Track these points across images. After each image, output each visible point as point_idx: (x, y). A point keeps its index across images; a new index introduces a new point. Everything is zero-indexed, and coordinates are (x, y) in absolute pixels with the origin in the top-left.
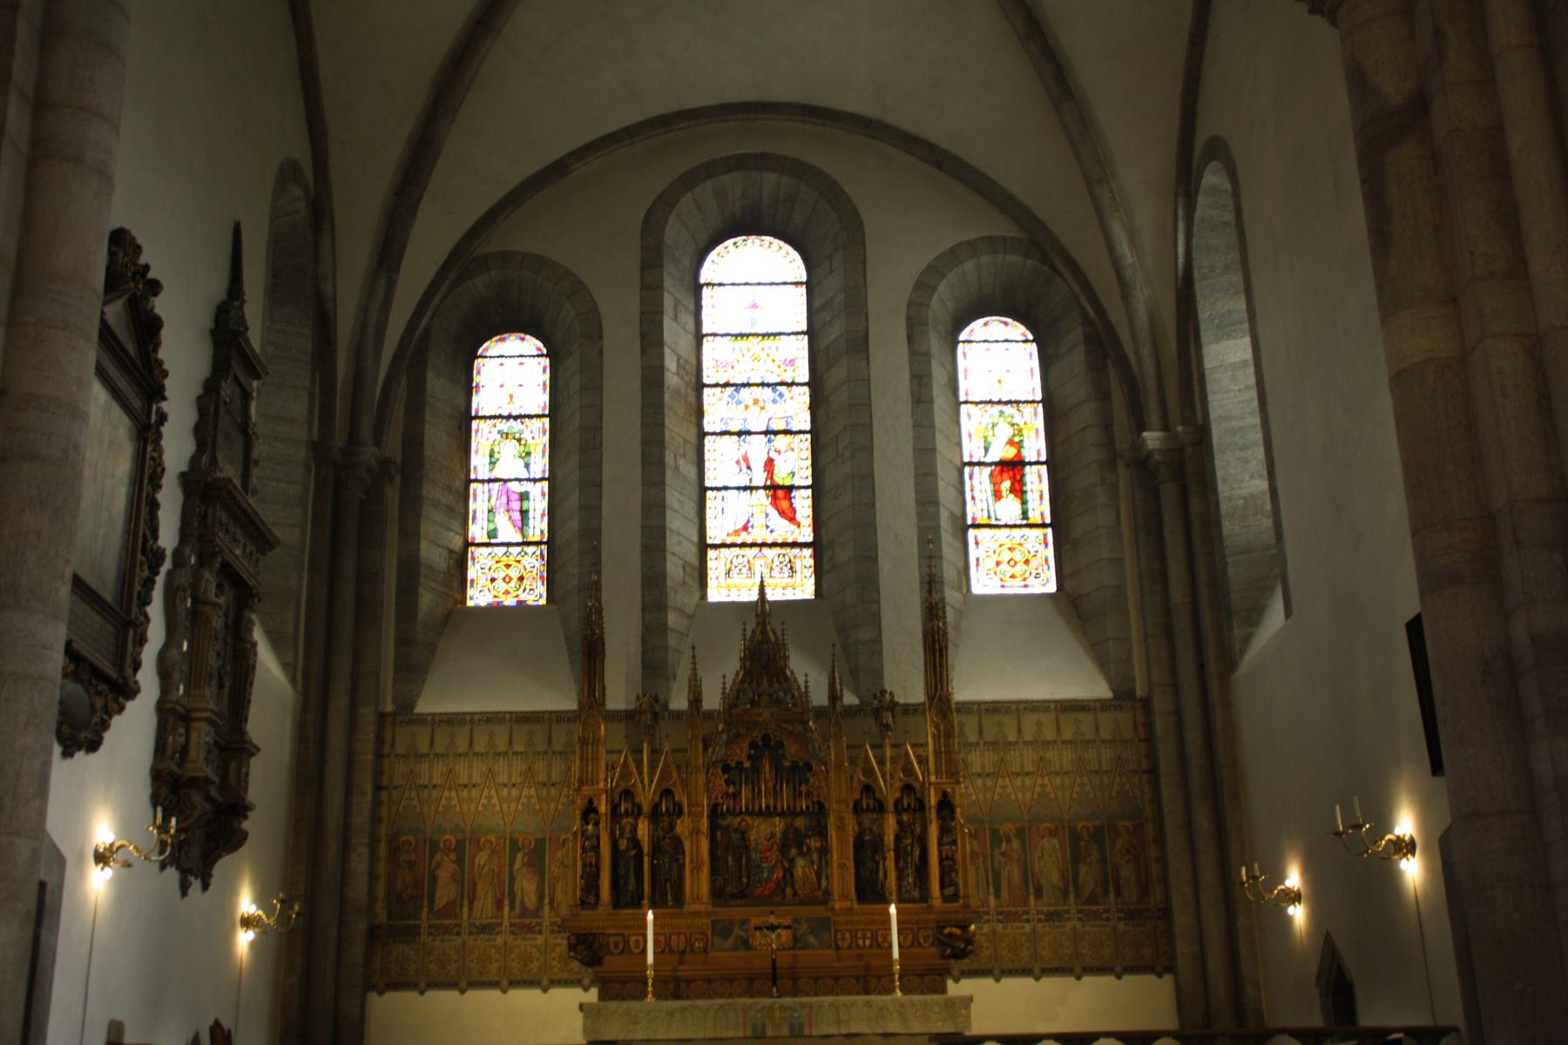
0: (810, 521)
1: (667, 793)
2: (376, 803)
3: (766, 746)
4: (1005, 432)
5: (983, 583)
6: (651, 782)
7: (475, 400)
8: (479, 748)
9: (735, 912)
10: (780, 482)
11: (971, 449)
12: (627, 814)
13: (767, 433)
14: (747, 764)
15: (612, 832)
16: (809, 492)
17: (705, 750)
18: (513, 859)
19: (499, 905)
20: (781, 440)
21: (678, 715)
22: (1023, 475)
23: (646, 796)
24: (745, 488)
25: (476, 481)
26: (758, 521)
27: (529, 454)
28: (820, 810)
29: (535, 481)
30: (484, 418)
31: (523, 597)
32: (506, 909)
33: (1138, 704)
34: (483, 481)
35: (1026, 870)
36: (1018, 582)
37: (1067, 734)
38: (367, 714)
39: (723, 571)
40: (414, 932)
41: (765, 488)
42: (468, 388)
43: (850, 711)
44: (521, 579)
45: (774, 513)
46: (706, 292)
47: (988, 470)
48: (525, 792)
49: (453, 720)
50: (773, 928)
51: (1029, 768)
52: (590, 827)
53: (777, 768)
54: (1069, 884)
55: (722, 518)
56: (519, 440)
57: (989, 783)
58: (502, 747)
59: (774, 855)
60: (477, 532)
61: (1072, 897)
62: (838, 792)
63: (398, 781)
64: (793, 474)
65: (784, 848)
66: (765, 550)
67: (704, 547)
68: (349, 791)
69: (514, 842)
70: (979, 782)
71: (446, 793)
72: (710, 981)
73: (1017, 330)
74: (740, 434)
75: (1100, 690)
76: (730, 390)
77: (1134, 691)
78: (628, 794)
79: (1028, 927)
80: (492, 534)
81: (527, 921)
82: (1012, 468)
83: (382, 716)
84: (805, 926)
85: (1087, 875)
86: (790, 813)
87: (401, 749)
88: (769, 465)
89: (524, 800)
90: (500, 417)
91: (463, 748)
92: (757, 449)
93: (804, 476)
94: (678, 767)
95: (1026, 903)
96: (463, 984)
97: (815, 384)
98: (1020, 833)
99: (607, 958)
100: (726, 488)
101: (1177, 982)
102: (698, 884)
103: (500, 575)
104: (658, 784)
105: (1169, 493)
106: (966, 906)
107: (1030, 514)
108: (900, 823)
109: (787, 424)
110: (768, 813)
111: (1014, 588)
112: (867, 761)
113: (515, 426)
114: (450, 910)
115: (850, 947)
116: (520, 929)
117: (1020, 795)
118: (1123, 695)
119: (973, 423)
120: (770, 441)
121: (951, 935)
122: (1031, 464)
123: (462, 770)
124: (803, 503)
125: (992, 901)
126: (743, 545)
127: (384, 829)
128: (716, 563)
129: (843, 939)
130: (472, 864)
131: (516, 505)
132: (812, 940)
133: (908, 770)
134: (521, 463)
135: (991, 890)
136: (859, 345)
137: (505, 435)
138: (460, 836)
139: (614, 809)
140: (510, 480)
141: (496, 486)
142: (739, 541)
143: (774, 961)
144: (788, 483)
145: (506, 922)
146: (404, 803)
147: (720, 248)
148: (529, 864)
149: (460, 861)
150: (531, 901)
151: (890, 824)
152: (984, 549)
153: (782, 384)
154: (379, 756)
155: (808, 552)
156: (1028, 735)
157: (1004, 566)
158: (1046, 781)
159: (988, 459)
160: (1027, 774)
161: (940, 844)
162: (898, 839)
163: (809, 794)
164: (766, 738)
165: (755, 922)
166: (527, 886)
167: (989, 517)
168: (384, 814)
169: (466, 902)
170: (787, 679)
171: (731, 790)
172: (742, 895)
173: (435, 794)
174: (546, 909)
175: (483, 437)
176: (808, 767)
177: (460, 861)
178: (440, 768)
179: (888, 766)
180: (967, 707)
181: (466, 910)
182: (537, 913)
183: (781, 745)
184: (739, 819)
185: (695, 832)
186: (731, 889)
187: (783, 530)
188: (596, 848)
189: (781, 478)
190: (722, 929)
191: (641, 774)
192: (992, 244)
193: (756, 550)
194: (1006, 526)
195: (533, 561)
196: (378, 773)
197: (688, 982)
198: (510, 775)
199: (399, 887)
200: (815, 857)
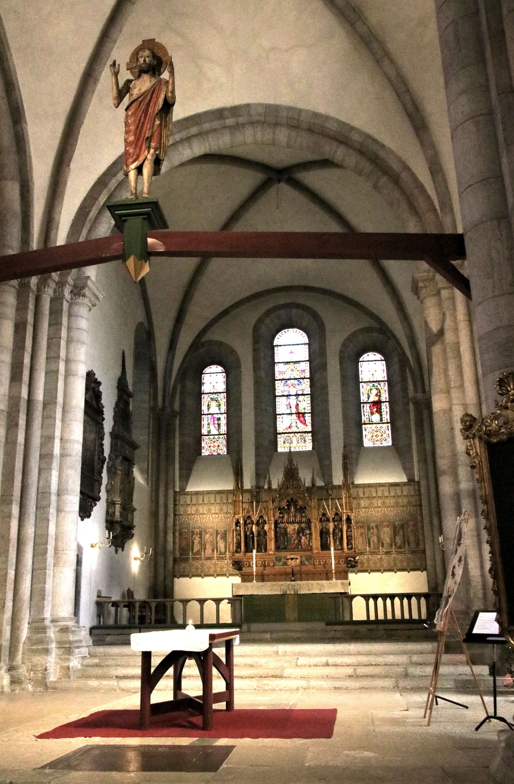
0: (310, 424)
1: (261, 517)
2: (175, 520)
3: (292, 502)
4: (374, 392)
5: (367, 443)
6: (256, 513)
7: (203, 388)
8: (206, 502)
9: (283, 554)
10: (300, 411)
11: (363, 398)
12: (249, 523)
13: (296, 395)
14: (286, 508)
15: (245, 529)
16: (310, 415)
17: (273, 502)
18: (217, 537)
19: (213, 551)
20: (301, 398)
21: (266, 490)
22: (381, 406)
23: (255, 518)
24: (289, 414)
25: (204, 414)
26: (294, 425)
27: (220, 405)
28: (309, 522)
29: (222, 414)
30: (206, 393)
31: (219, 452)
32: (215, 552)
33: (416, 484)
34: (206, 414)
35: (379, 538)
36: (378, 442)
37: (392, 494)
38: (171, 492)
39: (282, 442)
40: (187, 560)
41: (296, 413)
42: (200, 384)
43: (320, 488)
44: (219, 446)
45: (298, 422)
46: (275, 348)
47: (368, 405)
48: (220, 515)
49: (197, 493)
50: (292, 559)
51: (380, 505)
52: (238, 528)
53: (295, 507)
54: (393, 543)
55: (282, 425)
56: (217, 401)
57: (367, 510)
58: (213, 502)
59: (295, 536)
60: (204, 431)
61: (394, 546)
62: (314, 515)
63: (182, 513)
64: (305, 409)
65: (298, 533)
66: (296, 434)
67: (276, 434)
68: (166, 515)
69: (217, 531)
70: (364, 510)
71: (196, 516)
72: (274, 575)
73: (378, 356)
74: (287, 396)
75: (404, 479)
76: (284, 381)
77: (414, 478)
78: (249, 517)
79: (379, 557)
80: (209, 432)
81: (221, 556)
82: (377, 404)
83: (175, 493)
84: (304, 558)
85: (399, 540)
86: (300, 522)
87: (182, 502)
88: (297, 405)
89: (220, 518)
90: (211, 393)
91: (201, 502)
92: (293, 401)
93: (308, 409)
94: (265, 509)
95: (379, 549)
96: (203, 575)
97: (311, 378)
98: (377, 527)
99: (244, 568)
100: (283, 414)
101: (427, 573)
102: (271, 545)
103: (212, 445)
104: (259, 514)
106: (355, 551)
107: (383, 419)
108: (335, 525)
109: (303, 392)
110: (293, 523)
111: (378, 444)
112: (324, 506)
113: (215, 396)
114: (198, 553)
115: (318, 564)
116: (219, 558)
117: (377, 514)
118: (411, 480)
119: (364, 389)
120: (297, 398)
121: (350, 560)
122: (384, 402)
123: (201, 509)
124: (308, 418)
125: (368, 549)
126: (289, 433)
127: (177, 527)
128: (280, 439)
129: (316, 562)
130: (204, 539)
131: (216, 422)
132: (306, 562)
133: (337, 508)
134: (217, 408)
135: (368, 545)
136: (324, 367)
137: (212, 399)
138: (201, 530)
139: (245, 522)
140: (214, 414)
141: (210, 416)
142: (288, 431)
143: (293, 569)
144: (303, 411)
145: (215, 557)
146: (183, 520)
147: (280, 333)
148: (222, 538)
149: (201, 538)
150: (223, 550)
151: (331, 526)
152: (367, 431)
153: (301, 378)
154: (175, 505)
155: (310, 435)
156: (380, 494)
157: (374, 437)
158: (385, 509)
159: (369, 401)
160: (379, 507)
161: (347, 532)
162: (334, 530)
163: (305, 516)
164: (292, 499)
165: (289, 557)
166: (221, 545)
167: (369, 421)
168: (177, 524)
169: (203, 550)
170: (298, 480)
171: (281, 516)
172: (285, 549)
173: (192, 517)
174: (228, 552)
175: (205, 400)
176: (305, 508)
177: (201, 538)
178: (194, 508)
179: (330, 508)
181: (203, 552)
182: (225, 553)
183: (297, 501)
184: (284, 525)
185: (270, 529)
186: (282, 546)
187: (302, 427)
188: (240, 535)
189: (301, 410)
190: (279, 559)
191: (253, 511)
192: (368, 330)
193: (293, 434)
194: (375, 423)
196: (175, 511)
197: (268, 576)
198: (215, 510)
199: (183, 546)
200: (308, 536)
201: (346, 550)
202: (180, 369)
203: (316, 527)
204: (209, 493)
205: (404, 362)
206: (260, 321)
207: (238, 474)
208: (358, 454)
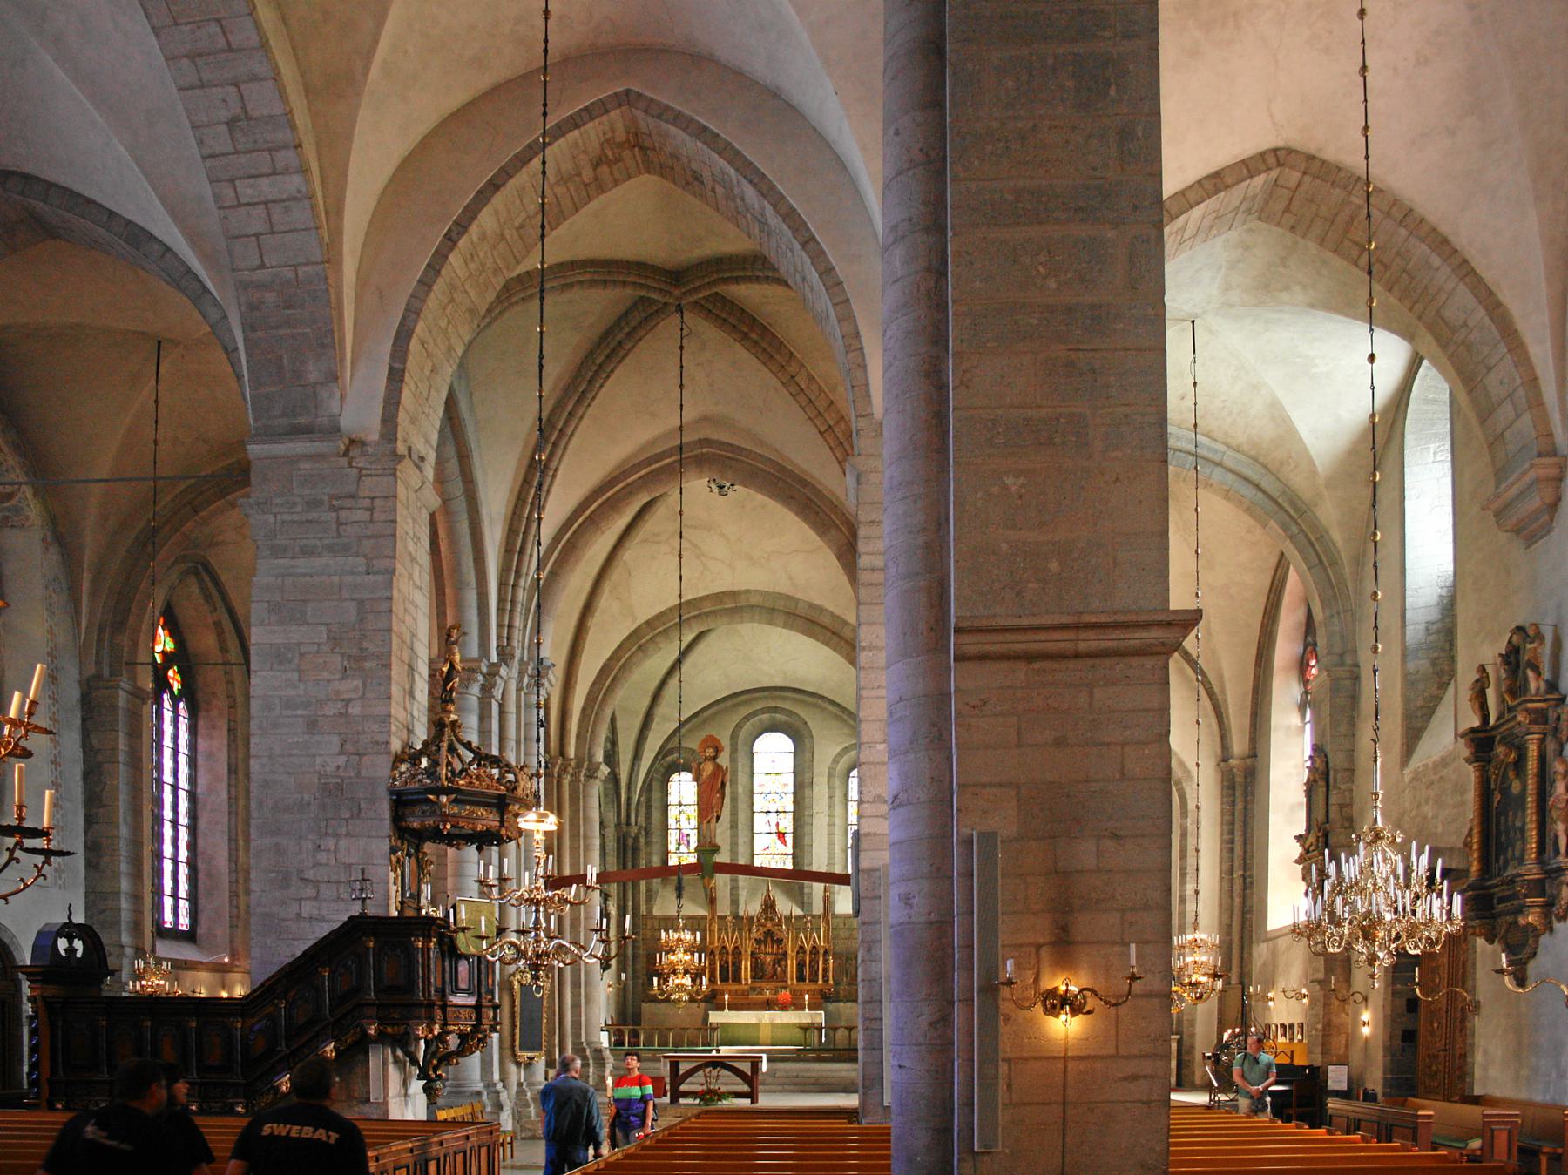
9: (758, 984)
28: (785, 954)
88: (777, 824)
92: (773, 817)
93: (790, 829)
124: (789, 838)
190: (753, 989)
201: (820, 982)
202: (645, 779)
206: (739, 727)
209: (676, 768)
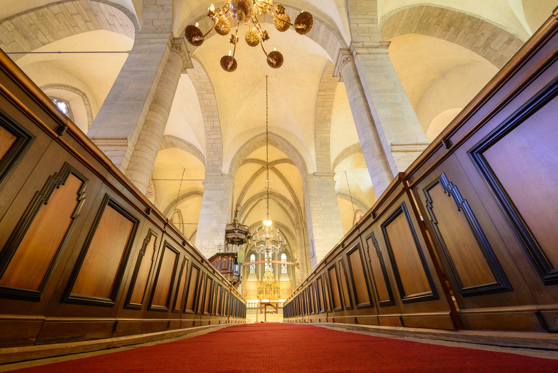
5: (282, 272)
9: (266, 295)
23: (261, 287)
38: (244, 281)
42: (250, 258)
49: (249, 282)
54: (287, 293)
60: (251, 268)
73: (285, 254)
85: (288, 293)
93: (271, 265)
102: (264, 293)
105: (293, 267)
114: (249, 294)
118: (291, 280)
151: (276, 289)
152: (282, 270)
166: (254, 293)
180: (280, 281)
195: (254, 271)
203: (273, 289)
204: (252, 282)
205: (290, 256)
207: (258, 278)
208: (281, 274)
209: (251, 254)
